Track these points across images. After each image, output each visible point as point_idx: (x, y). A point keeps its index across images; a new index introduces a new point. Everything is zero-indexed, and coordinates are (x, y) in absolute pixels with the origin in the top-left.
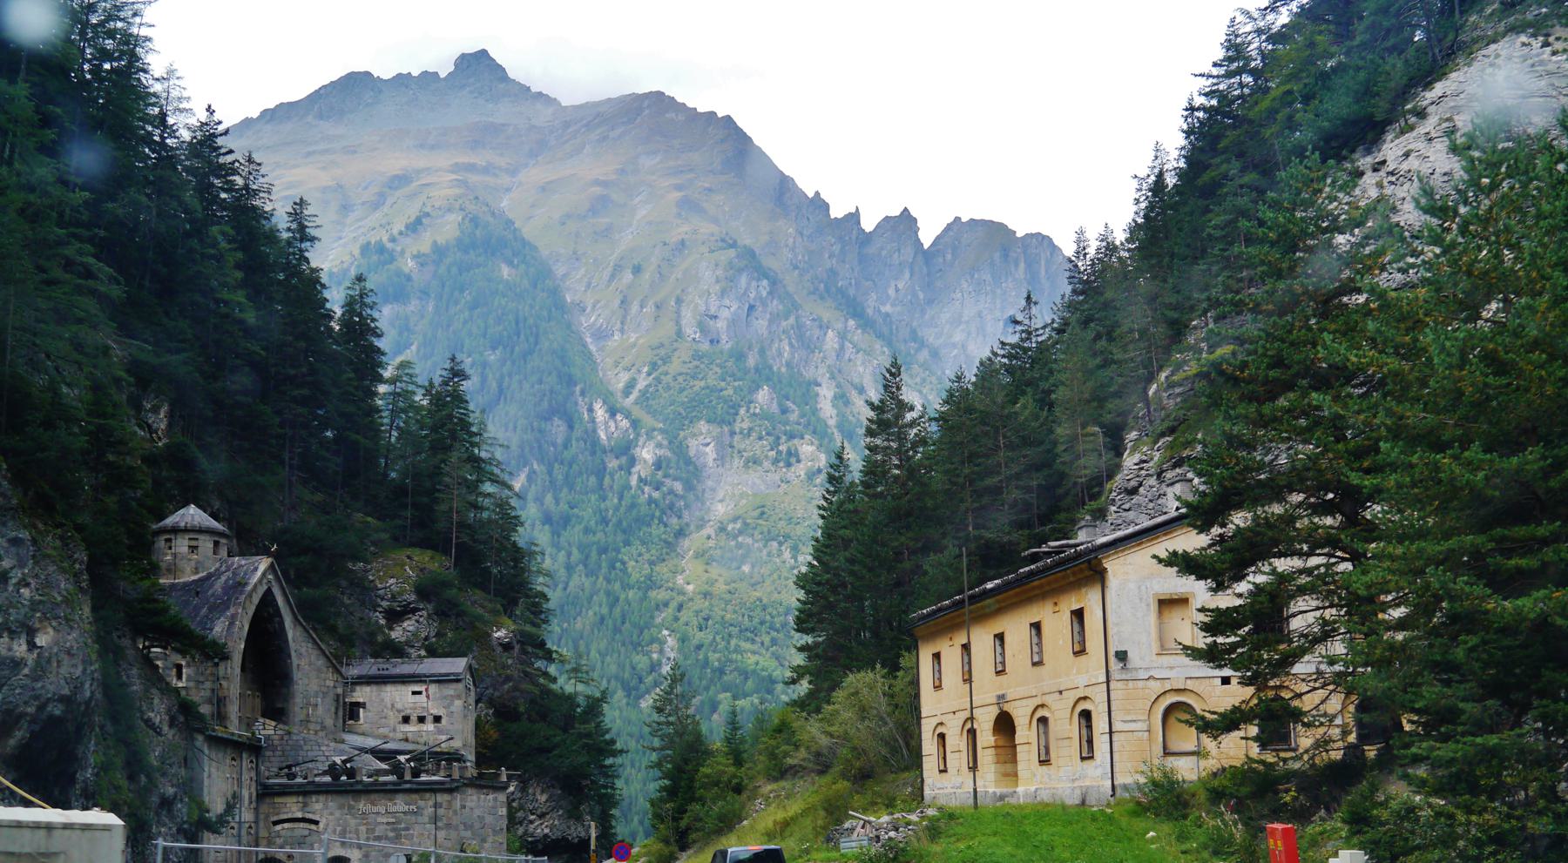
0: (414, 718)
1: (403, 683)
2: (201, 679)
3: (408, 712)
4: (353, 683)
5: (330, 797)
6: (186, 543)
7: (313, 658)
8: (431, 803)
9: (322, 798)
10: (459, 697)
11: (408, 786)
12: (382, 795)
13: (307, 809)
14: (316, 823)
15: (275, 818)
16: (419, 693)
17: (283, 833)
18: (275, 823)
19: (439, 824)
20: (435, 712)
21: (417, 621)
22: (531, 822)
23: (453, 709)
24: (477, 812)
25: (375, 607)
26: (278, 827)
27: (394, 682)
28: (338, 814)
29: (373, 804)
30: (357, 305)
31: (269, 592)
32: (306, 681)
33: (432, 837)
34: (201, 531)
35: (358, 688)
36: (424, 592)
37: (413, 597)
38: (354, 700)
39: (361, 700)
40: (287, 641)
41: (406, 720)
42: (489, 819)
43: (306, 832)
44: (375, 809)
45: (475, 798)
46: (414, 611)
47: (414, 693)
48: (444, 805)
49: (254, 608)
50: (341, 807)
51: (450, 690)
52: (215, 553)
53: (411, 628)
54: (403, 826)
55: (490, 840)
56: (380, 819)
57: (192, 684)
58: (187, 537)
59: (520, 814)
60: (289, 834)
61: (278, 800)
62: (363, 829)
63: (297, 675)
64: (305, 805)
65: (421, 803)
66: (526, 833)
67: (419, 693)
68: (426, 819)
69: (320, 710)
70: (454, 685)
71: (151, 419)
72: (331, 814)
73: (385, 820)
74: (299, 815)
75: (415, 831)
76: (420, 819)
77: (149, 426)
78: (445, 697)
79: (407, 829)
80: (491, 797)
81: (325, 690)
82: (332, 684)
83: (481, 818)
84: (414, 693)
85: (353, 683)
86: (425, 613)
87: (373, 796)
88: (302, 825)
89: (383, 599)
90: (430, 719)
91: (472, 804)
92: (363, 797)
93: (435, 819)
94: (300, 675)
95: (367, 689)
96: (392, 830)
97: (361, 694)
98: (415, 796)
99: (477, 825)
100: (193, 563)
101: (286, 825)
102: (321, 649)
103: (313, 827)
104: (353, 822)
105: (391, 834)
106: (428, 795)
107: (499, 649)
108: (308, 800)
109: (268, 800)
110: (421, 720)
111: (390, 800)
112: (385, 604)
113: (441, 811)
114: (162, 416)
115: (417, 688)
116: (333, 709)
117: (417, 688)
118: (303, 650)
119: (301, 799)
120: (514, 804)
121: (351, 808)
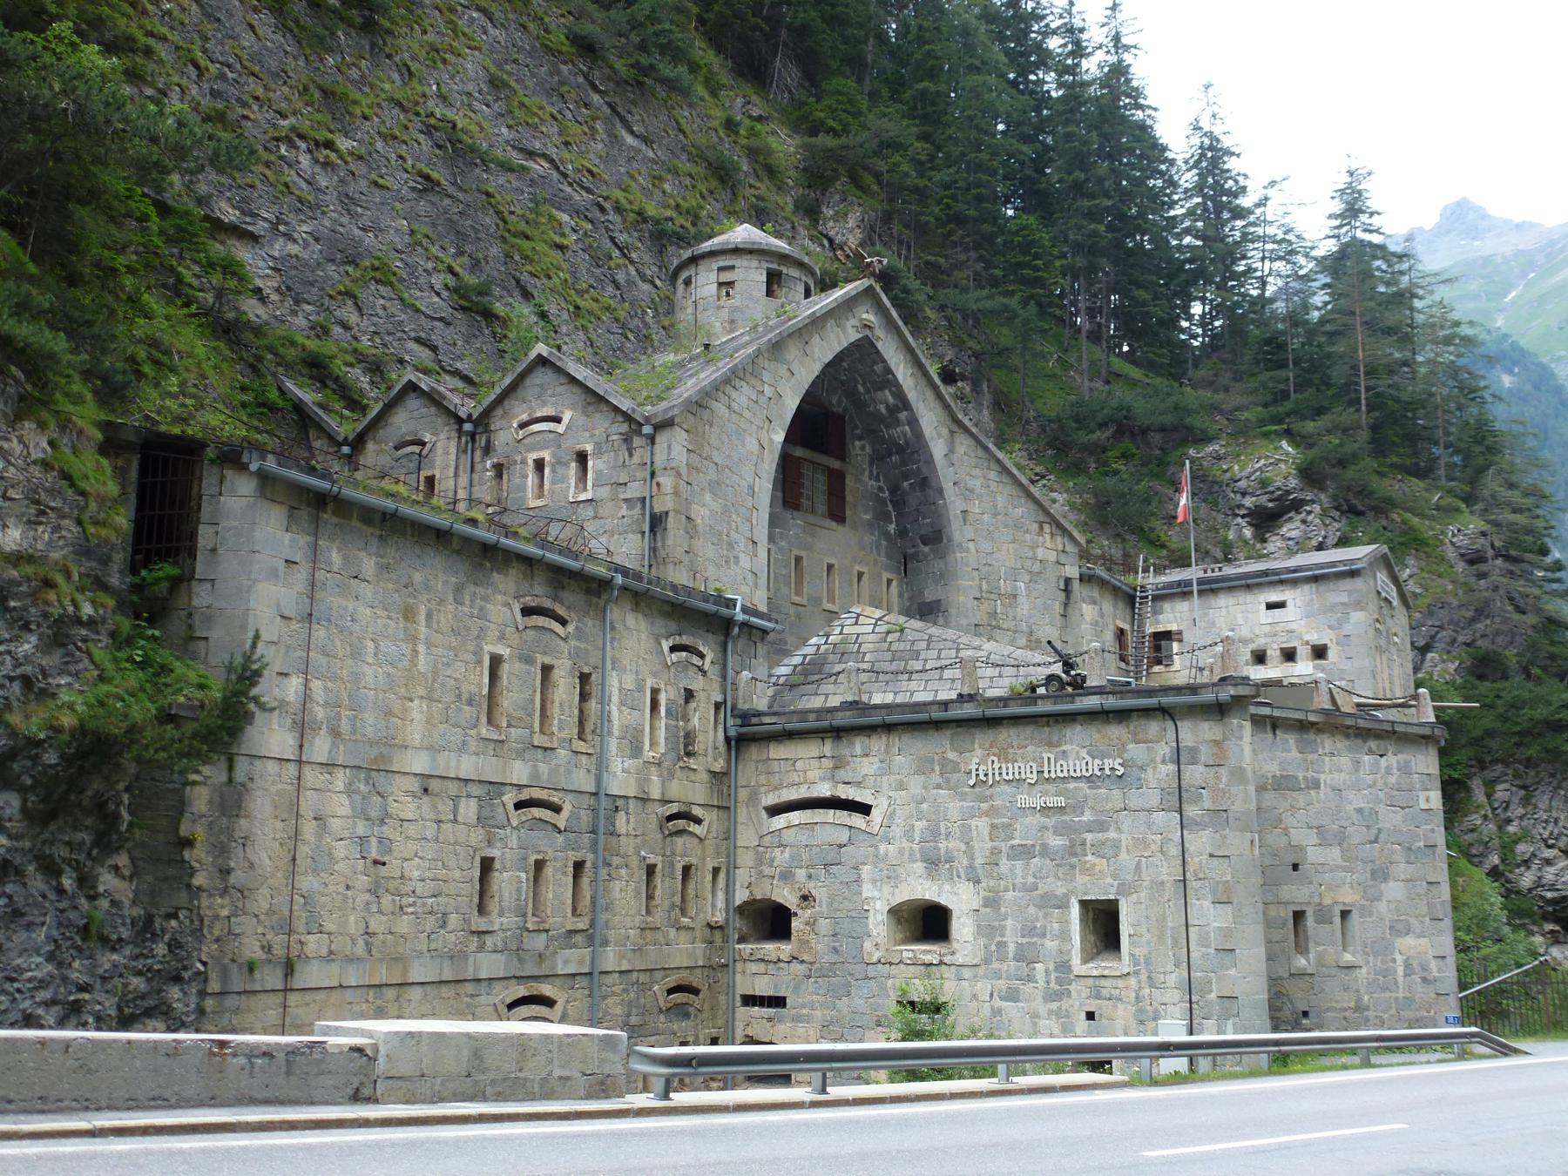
0: (1273, 653)
1: (1248, 587)
2: (623, 479)
3: (1259, 643)
4: (1156, 598)
5: (895, 740)
6: (713, 276)
7: (1001, 501)
8: (1164, 749)
9: (877, 743)
10: (1358, 605)
11: (1092, 702)
12: (1028, 731)
13: (843, 774)
14: (865, 809)
15: (771, 799)
16: (1281, 605)
17: (789, 836)
18: (775, 811)
19: (1191, 811)
20: (1315, 638)
21: (1304, 522)
22: (1548, 862)
23: (1348, 629)
24: (1355, 800)
25: (1233, 511)
26: (780, 821)
27: (1231, 589)
28: (916, 785)
29: (1003, 756)
30: (1212, 158)
31: (864, 350)
32: (986, 545)
33: (1174, 850)
34: (737, 251)
35: (1167, 606)
36: (1309, 475)
37: (1293, 483)
38: (1161, 628)
39: (1174, 627)
40: (930, 461)
41: (1260, 658)
42: (1391, 819)
43: (843, 836)
44: (1011, 770)
45: (1345, 761)
46: (1297, 505)
47: (1270, 606)
48: (1205, 753)
49: (816, 369)
50: (923, 768)
51: (1339, 594)
52: (768, 295)
53: (1293, 534)
54: (1088, 816)
55: (1402, 869)
56: (1024, 799)
57: (604, 492)
58: (715, 266)
59: (1523, 849)
60: (803, 838)
61: (777, 751)
62: (981, 825)
63: (959, 532)
64: (839, 763)
65: (1136, 751)
66: (1539, 883)
67: (1281, 605)
68: (1154, 799)
69: (1024, 606)
70: (1348, 584)
71: (832, 229)
72: (901, 787)
73: (1038, 802)
74: (824, 790)
75: (1126, 831)
76: (1135, 800)
77: (831, 241)
78: (1332, 609)
79: (1101, 826)
80: (1392, 760)
81: (1037, 567)
82: (1052, 556)
83: (1367, 816)
84: (1270, 606)
85: (1156, 598)
86: (1317, 508)
87: (1005, 735)
88: (830, 815)
89: (1244, 494)
90: (1303, 652)
91: (1340, 778)
92: (982, 738)
93: (1179, 797)
94: (969, 532)
95: (1182, 607)
96: (1057, 832)
97: (1171, 617)
98: (1116, 731)
99: (1356, 834)
100: (725, 314)
101: (795, 817)
102: (998, 461)
103: (857, 820)
104: (954, 807)
105: (1057, 842)
106: (1153, 727)
107: (1461, 566)
108: (844, 749)
109: (754, 752)
110: (1289, 655)
111: (1051, 745)
112: (1249, 502)
113: (1194, 774)
114: (851, 223)
115: (1275, 597)
116: (1058, 608)
117: (1275, 597)
118: (977, 484)
119: (828, 748)
120: (1511, 829)
121: (948, 767)
